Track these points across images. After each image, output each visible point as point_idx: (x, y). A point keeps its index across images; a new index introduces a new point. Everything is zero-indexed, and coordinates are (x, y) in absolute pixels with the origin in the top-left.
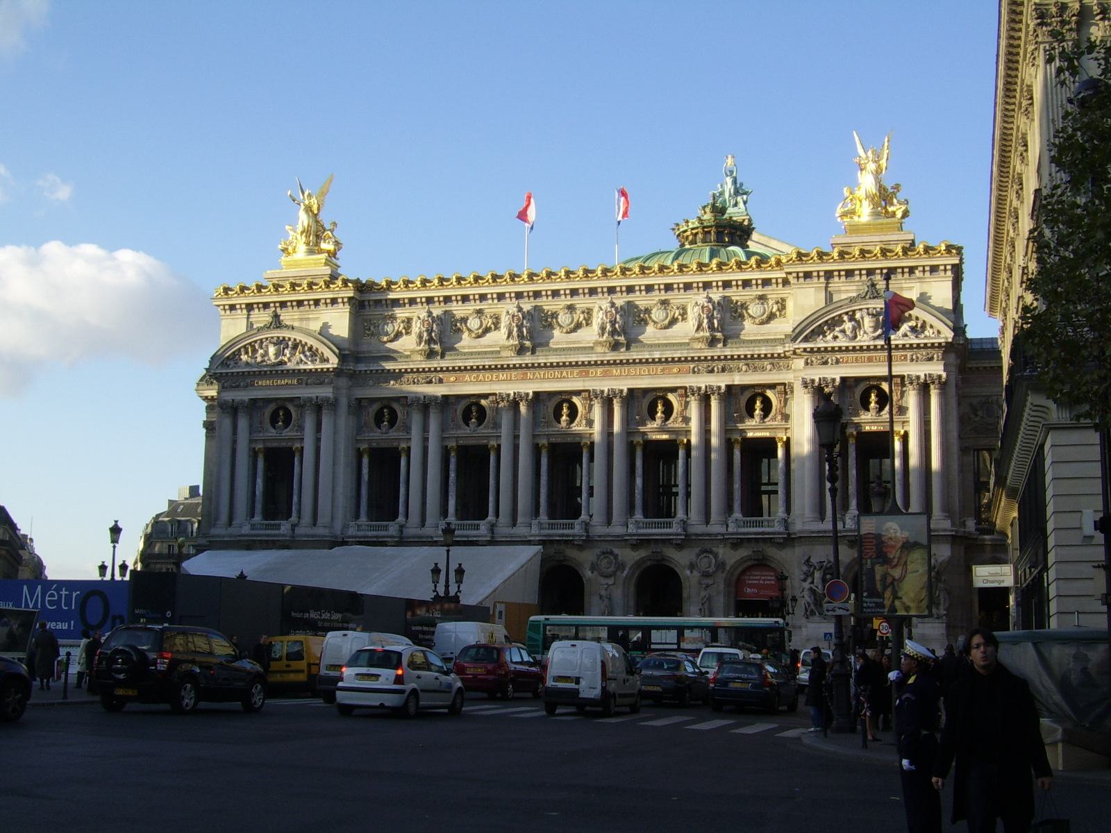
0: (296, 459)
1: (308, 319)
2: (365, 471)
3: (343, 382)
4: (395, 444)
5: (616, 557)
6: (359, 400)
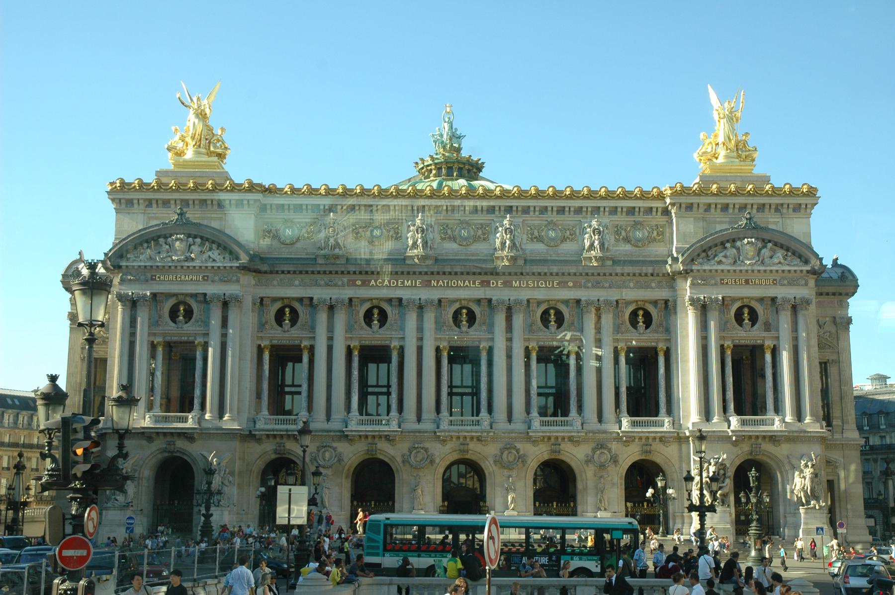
0: (198, 353)
1: (211, 218)
2: (266, 367)
3: (248, 279)
4: (297, 342)
5: (518, 451)
6: (262, 299)
